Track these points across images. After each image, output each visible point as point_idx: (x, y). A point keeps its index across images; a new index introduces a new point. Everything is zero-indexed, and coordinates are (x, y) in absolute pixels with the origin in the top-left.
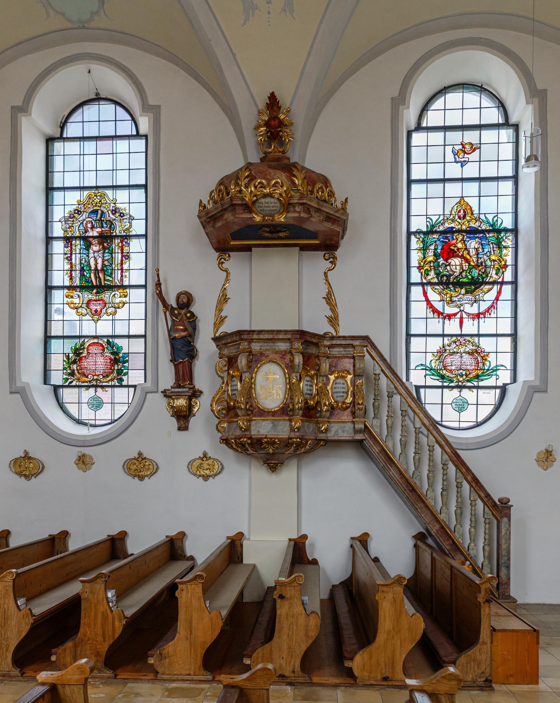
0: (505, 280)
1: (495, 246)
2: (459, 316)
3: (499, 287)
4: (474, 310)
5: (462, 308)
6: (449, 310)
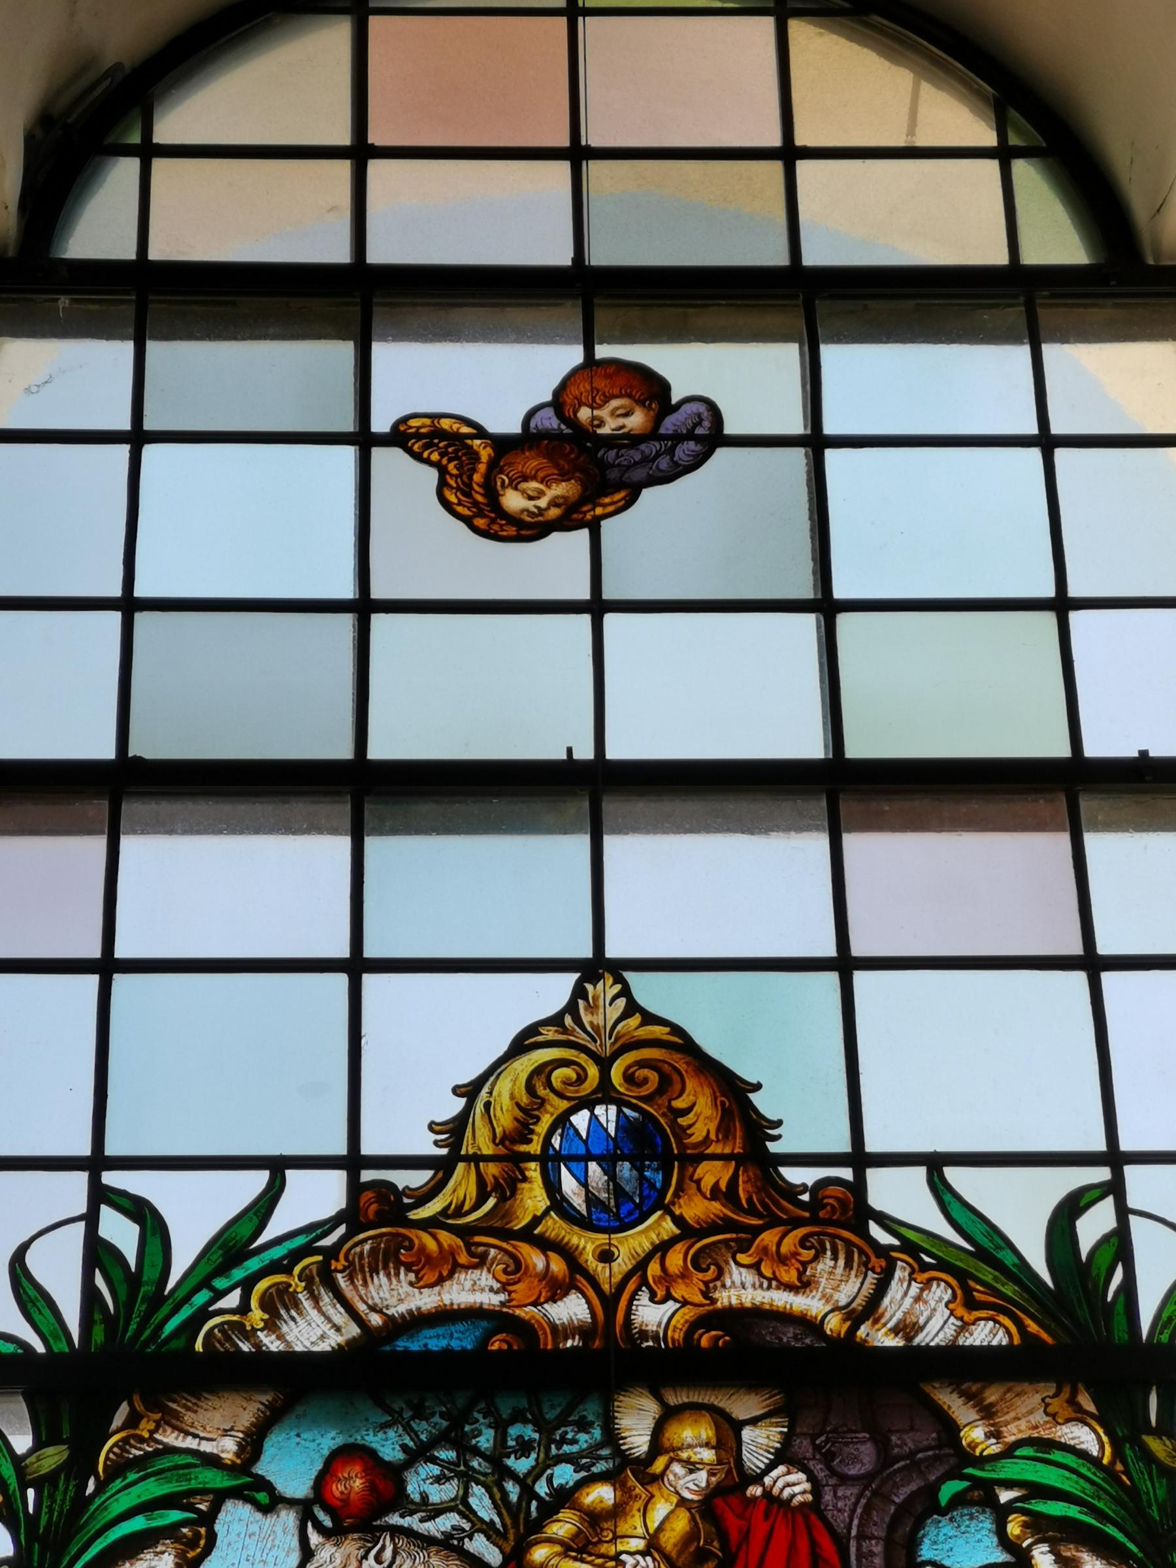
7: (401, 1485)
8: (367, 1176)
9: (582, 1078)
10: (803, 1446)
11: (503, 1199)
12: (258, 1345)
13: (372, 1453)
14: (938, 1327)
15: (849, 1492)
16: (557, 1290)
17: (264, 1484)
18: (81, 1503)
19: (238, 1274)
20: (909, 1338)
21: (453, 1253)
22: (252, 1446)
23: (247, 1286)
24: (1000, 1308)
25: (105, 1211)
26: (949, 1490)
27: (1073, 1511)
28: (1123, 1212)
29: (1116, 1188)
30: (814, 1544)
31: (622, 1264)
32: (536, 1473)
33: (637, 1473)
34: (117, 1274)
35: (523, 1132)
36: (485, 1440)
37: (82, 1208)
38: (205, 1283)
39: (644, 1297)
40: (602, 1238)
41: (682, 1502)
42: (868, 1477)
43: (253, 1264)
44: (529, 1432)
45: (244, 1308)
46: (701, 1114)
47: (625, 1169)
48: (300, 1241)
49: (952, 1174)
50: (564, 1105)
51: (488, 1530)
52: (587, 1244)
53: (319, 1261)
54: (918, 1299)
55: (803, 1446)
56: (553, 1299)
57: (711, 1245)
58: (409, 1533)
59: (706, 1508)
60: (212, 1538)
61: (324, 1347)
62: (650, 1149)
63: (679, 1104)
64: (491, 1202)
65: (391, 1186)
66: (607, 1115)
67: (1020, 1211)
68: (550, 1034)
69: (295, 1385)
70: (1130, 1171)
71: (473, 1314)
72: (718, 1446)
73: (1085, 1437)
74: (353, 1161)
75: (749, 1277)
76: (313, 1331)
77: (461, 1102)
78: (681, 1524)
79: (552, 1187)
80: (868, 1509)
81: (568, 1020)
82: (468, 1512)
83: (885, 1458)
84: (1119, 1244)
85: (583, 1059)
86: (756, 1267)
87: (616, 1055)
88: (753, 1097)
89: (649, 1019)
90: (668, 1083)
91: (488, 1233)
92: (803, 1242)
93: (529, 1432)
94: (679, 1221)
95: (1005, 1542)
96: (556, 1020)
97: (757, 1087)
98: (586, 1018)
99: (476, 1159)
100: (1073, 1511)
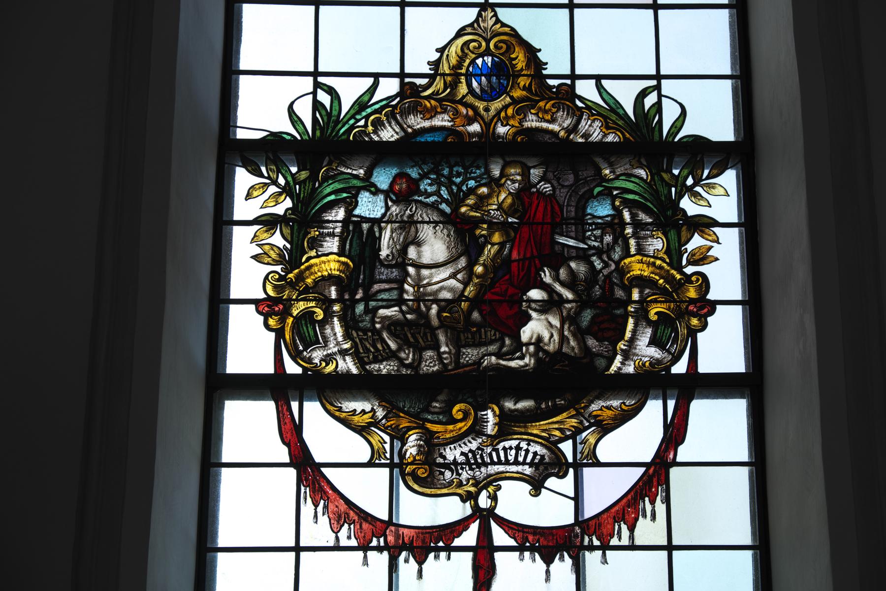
0: (703, 368)
1: (643, 217)
2: (469, 537)
3: (671, 404)
4: (551, 509)
5: (484, 501)
6: (420, 511)
7: (419, 186)
8: (407, 80)
9: (480, 46)
10: (550, 175)
11: (452, 90)
12: (371, 138)
13: (409, 175)
14: (596, 136)
15: (564, 190)
16: (470, 121)
17: (375, 186)
18: (314, 190)
19: (364, 114)
20: (587, 139)
21: (435, 107)
22: (369, 174)
23: (367, 117)
24: (616, 128)
25: (319, 91)
26: (598, 190)
27: (637, 198)
28: (660, 96)
29: (658, 88)
30: (553, 208)
31: (492, 112)
32: (462, 183)
33: (496, 184)
34: (324, 113)
35: (459, 65)
36: (446, 172)
37: (311, 90)
38: (353, 117)
39: (499, 125)
40: (485, 104)
41: (510, 193)
42: (571, 186)
43: (369, 110)
44: (461, 170)
45: (366, 126)
46: (520, 59)
47: (494, 79)
48: (384, 103)
49: (605, 83)
50: (474, 56)
51: (446, 201)
52: (481, 105)
53: (393, 110)
54: (590, 126)
55: (550, 175)
56: (469, 124)
57: (523, 107)
58: (420, 202)
59: (517, 196)
60: (357, 202)
61: (392, 139)
62: (502, 71)
63: (513, 56)
64: (449, 90)
65: (414, 84)
66: (488, 60)
67: (625, 95)
68: (469, 30)
69: (382, 153)
70: (663, 82)
71: (442, 128)
72: (522, 175)
73: (642, 173)
74: (402, 75)
75: (534, 118)
76: (388, 134)
77: (438, 55)
78: (509, 200)
79: (469, 85)
80: (570, 196)
81: (476, 25)
82: (440, 196)
83: (577, 179)
84: (658, 107)
85: (480, 39)
86: (537, 114)
87: (492, 38)
88: (538, 54)
89: (504, 25)
90: (510, 49)
91: (447, 101)
92: (553, 106)
93: (461, 170)
94: (512, 98)
95: (614, 207)
96: (471, 25)
97: (540, 50)
98: (482, 25)
99: (444, 75)
100: (637, 198)
